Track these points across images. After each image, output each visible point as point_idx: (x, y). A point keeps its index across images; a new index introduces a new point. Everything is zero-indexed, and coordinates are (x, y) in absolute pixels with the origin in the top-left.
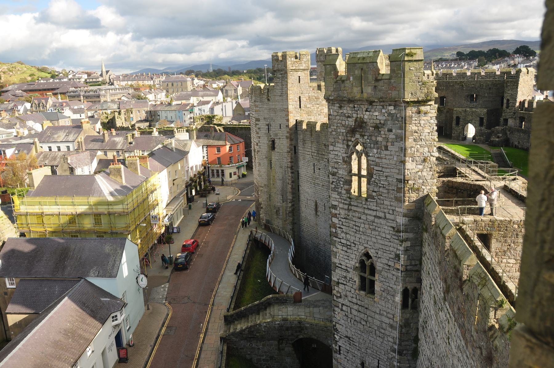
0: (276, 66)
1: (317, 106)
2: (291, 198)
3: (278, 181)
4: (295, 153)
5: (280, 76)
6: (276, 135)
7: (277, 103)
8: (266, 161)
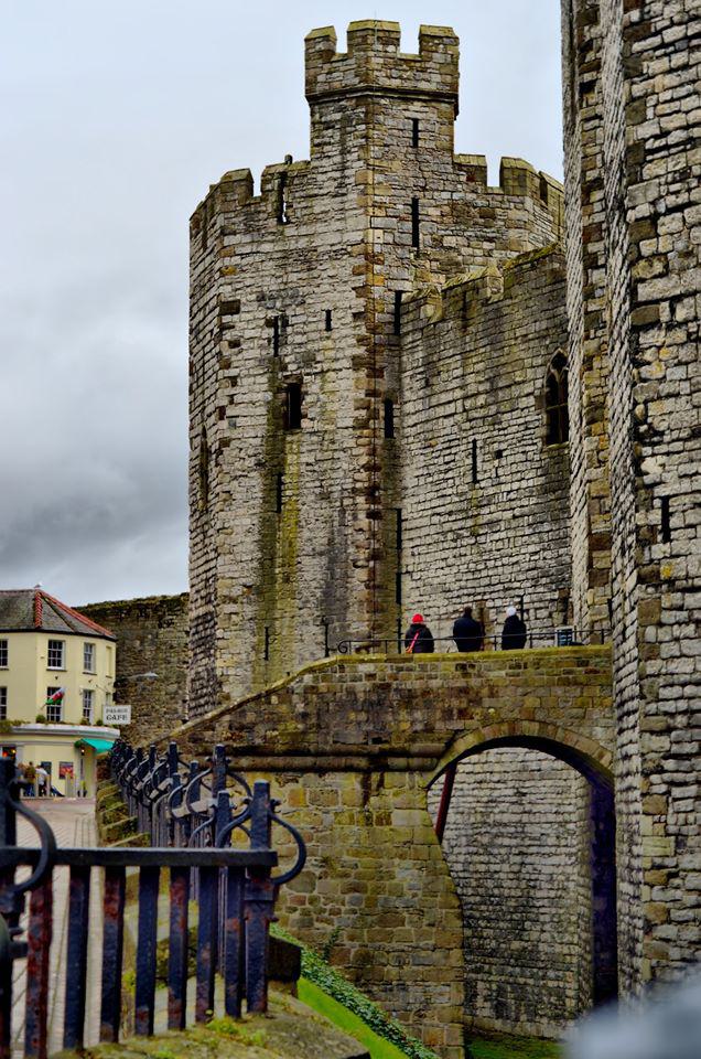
0: (321, 78)
1: (487, 245)
2: (364, 628)
3: (306, 561)
4: (390, 430)
5: (338, 116)
6: (309, 360)
7: (320, 227)
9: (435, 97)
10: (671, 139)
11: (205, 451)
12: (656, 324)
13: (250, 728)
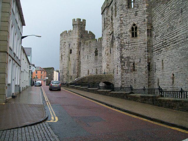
6: (72, 48)
8: (67, 58)
9: (84, 25)
10: (125, 33)
11: (62, 55)
12: (123, 48)
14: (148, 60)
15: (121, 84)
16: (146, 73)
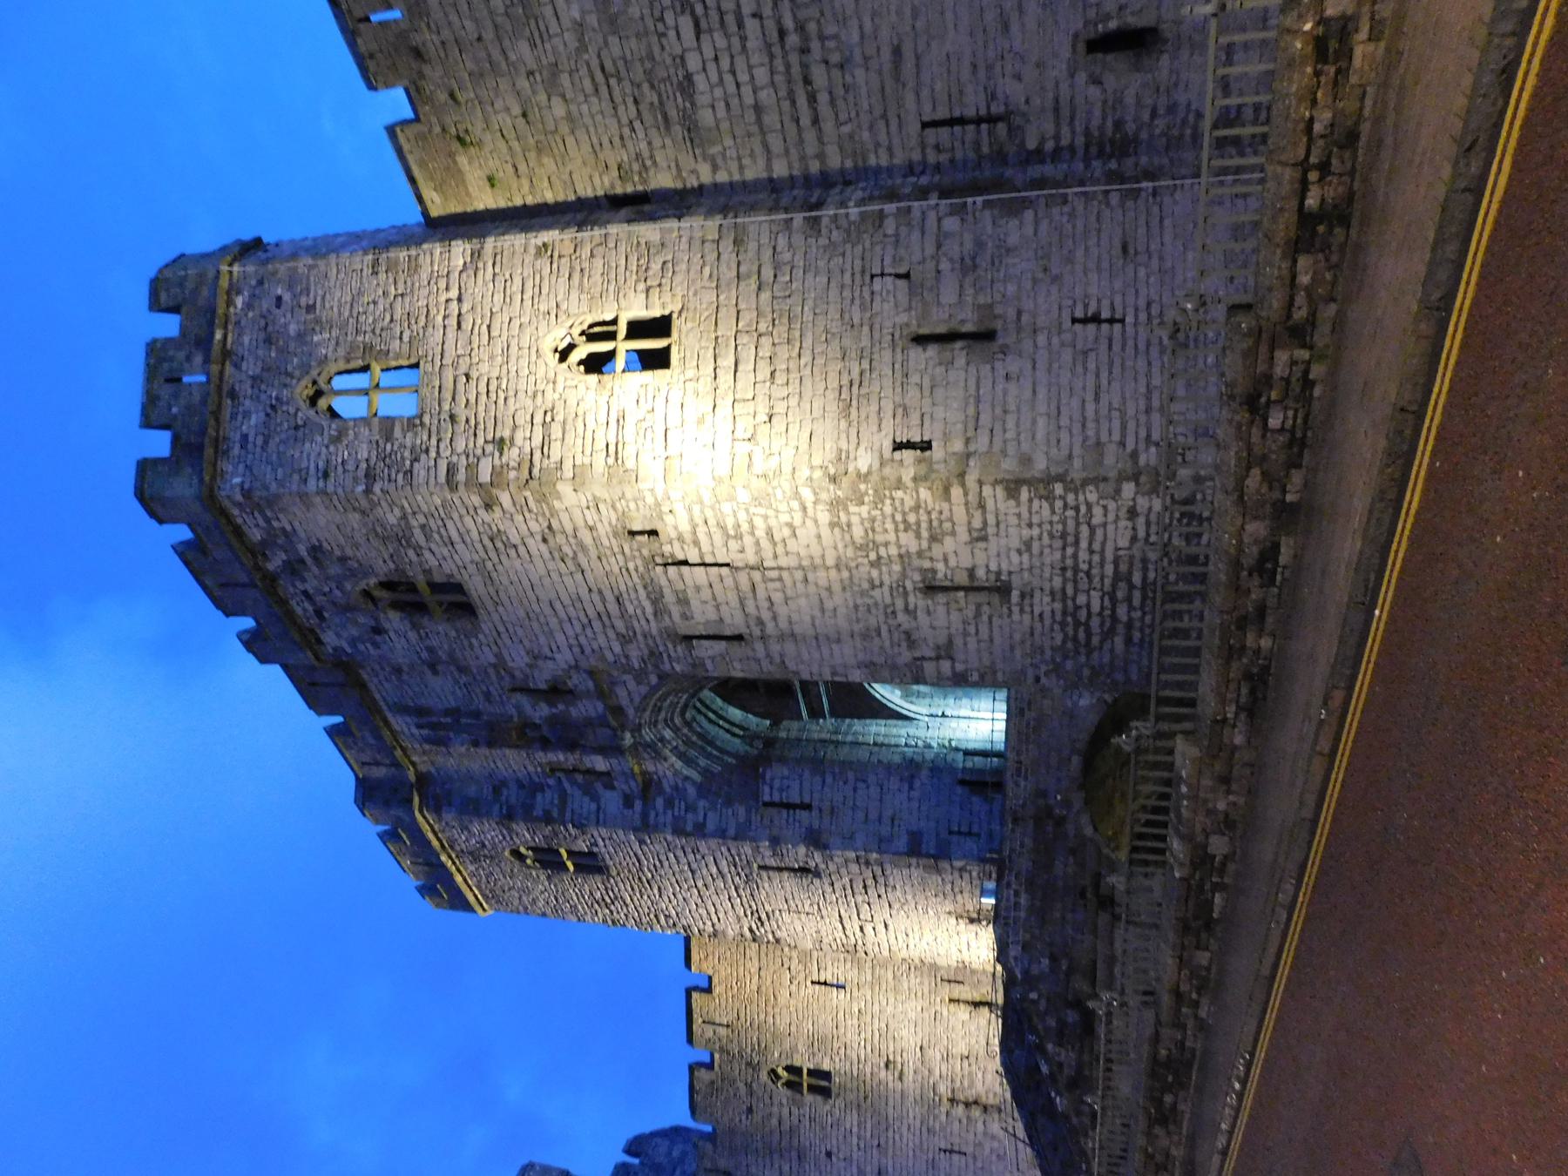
13: (1062, 1024)
14: (892, 196)
15: (1128, 489)
16: (1027, 203)
